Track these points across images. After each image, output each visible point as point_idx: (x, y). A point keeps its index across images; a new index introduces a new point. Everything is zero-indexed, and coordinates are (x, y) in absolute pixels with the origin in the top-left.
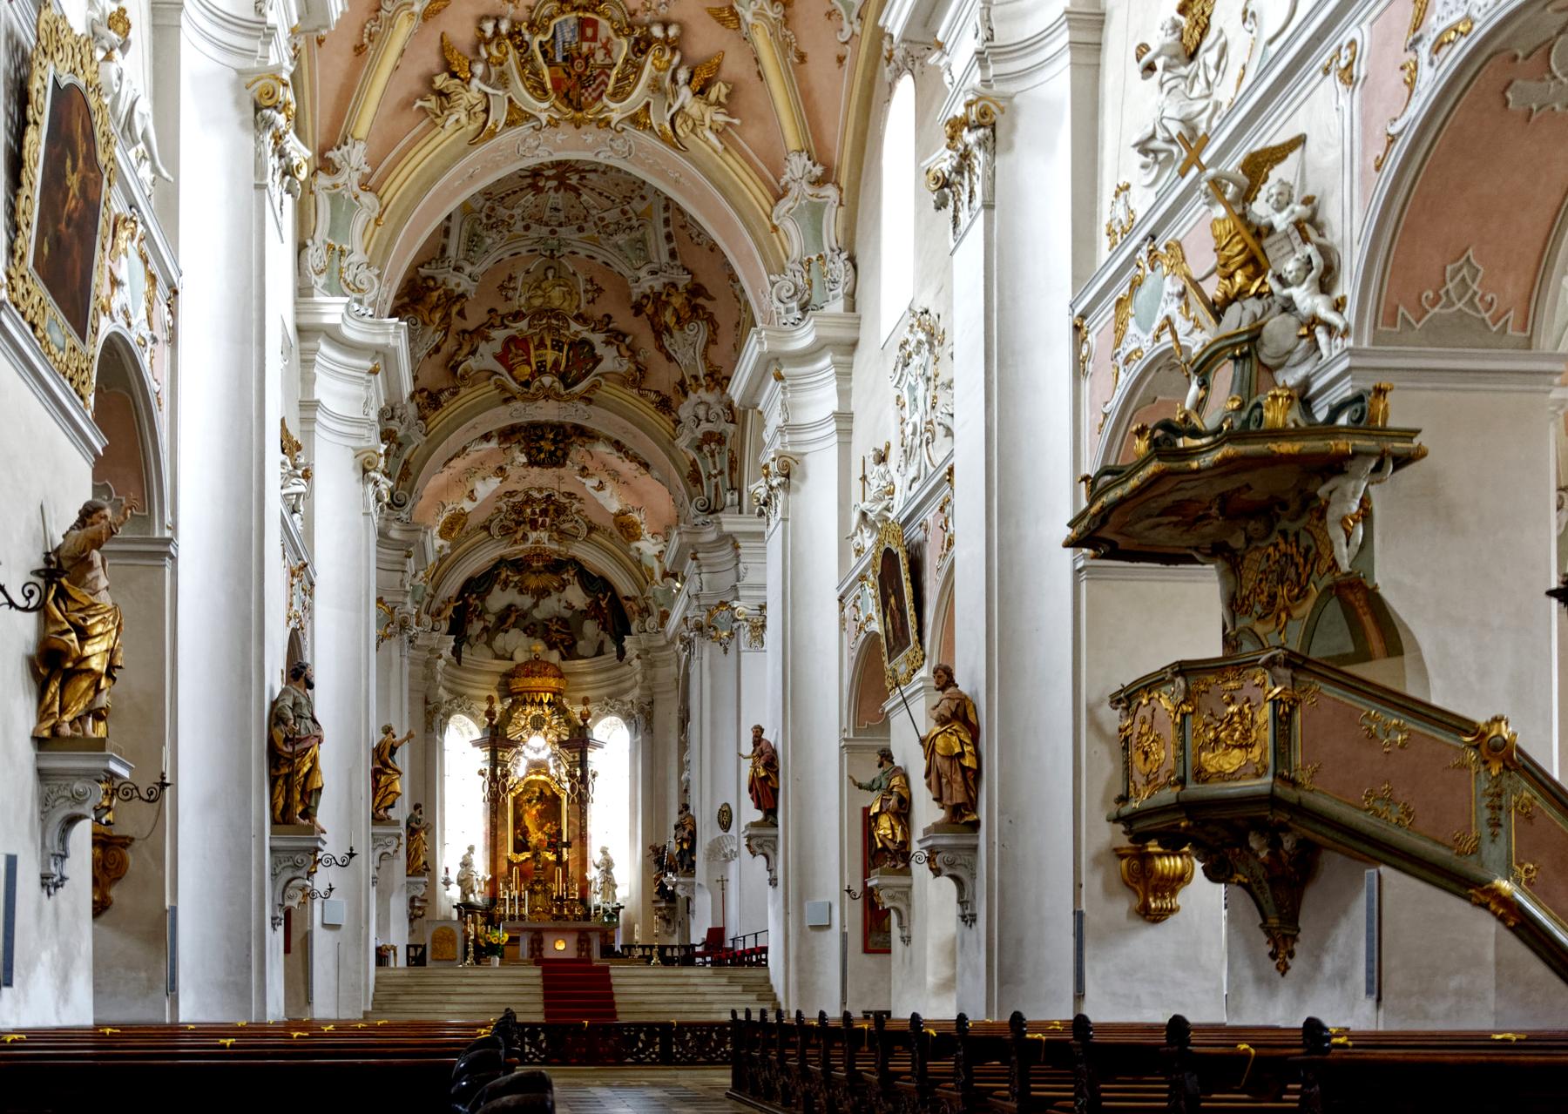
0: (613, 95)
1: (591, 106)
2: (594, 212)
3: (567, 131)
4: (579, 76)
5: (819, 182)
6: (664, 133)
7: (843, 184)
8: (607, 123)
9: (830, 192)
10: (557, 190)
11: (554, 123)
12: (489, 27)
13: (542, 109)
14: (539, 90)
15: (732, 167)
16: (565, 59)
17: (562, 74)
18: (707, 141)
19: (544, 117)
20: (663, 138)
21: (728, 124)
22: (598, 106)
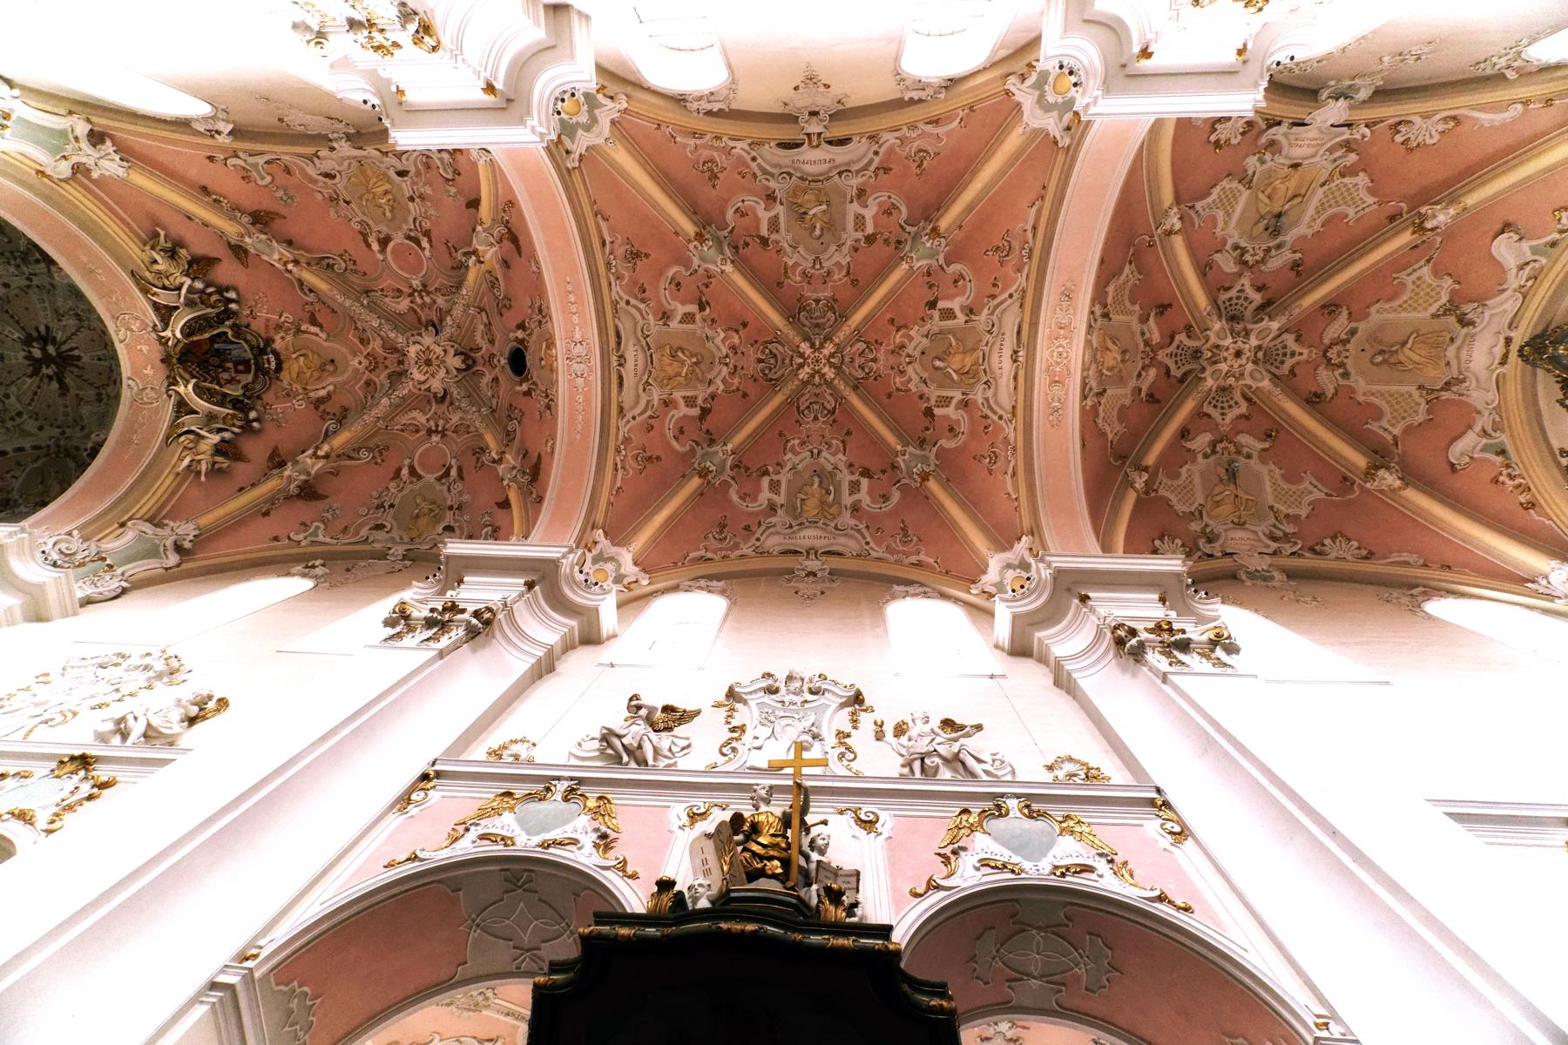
0: (196, 387)
1: (185, 370)
2: (14, 388)
3: (149, 349)
4: (207, 361)
5: (178, 548)
6: (178, 426)
7: (184, 566)
8: (175, 383)
9: (173, 559)
10: (29, 357)
11: (163, 341)
12: (232, 295)
13: (175, 331)
14: (189, 330)
15: (165, 482)
16: (217, 350)
17: (205, 348)
18: (181, 459)
19: (168, 333)
20: (173, 425)
21: (199, 473)
22: (187, 376)
